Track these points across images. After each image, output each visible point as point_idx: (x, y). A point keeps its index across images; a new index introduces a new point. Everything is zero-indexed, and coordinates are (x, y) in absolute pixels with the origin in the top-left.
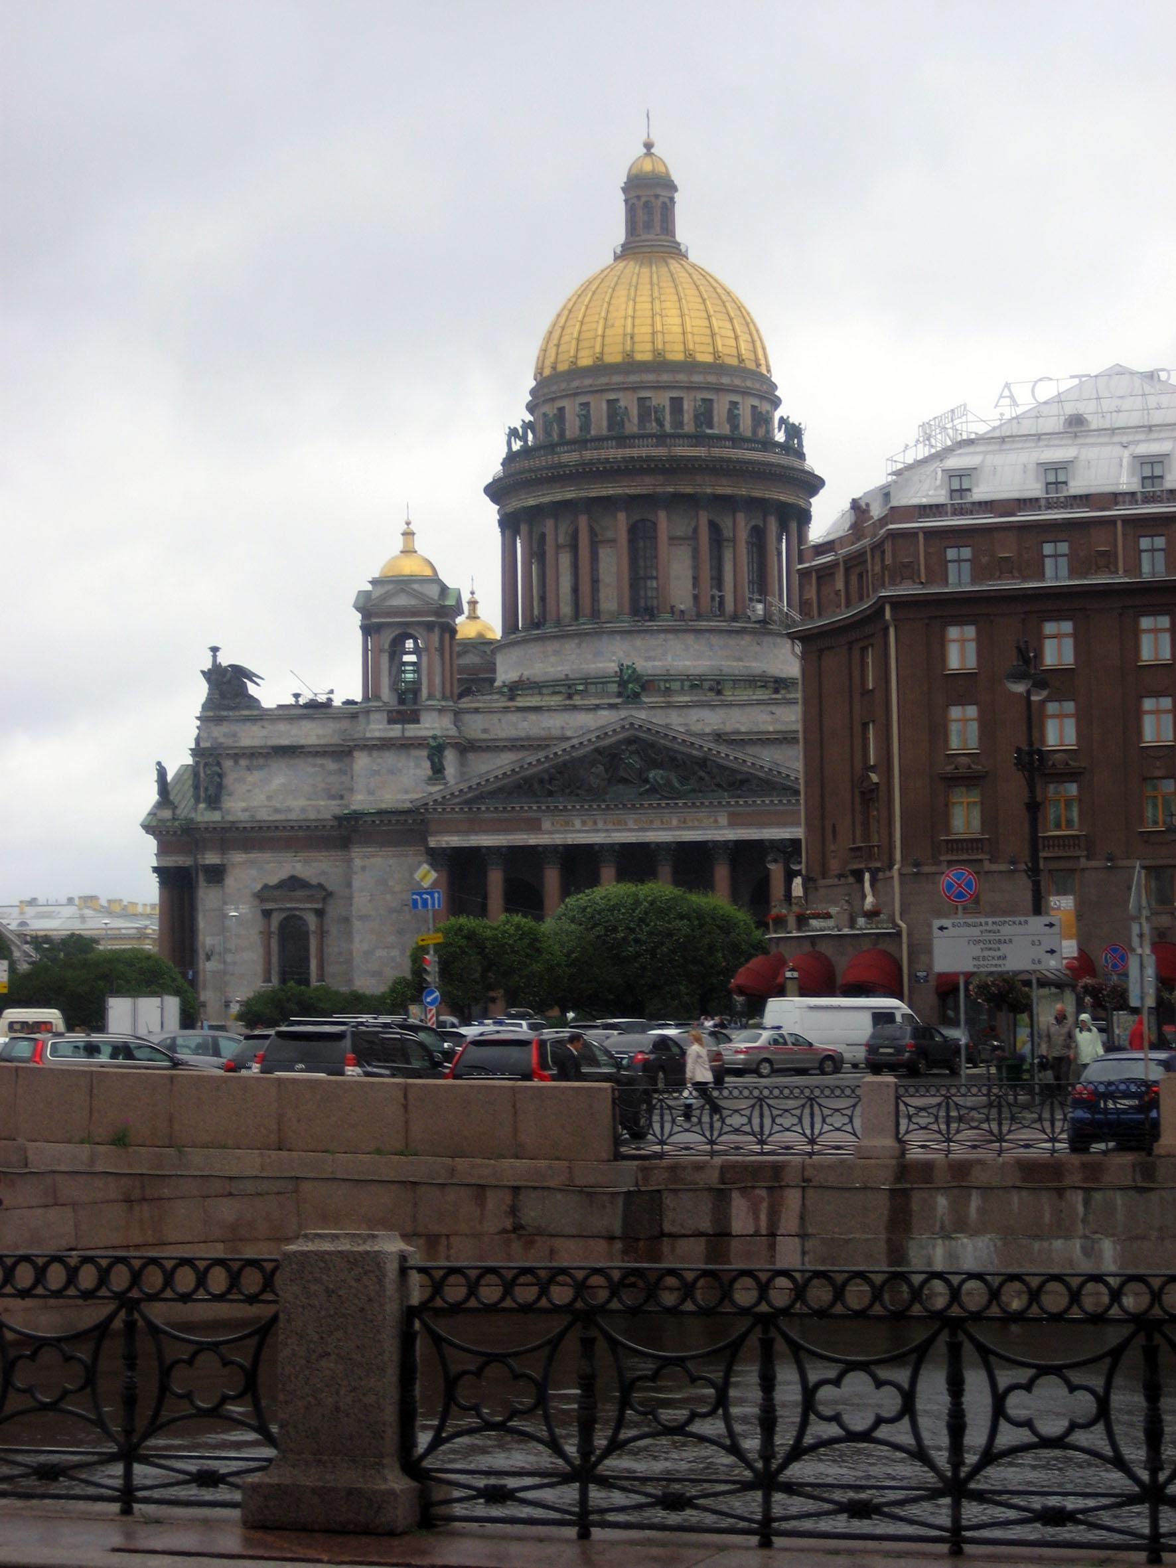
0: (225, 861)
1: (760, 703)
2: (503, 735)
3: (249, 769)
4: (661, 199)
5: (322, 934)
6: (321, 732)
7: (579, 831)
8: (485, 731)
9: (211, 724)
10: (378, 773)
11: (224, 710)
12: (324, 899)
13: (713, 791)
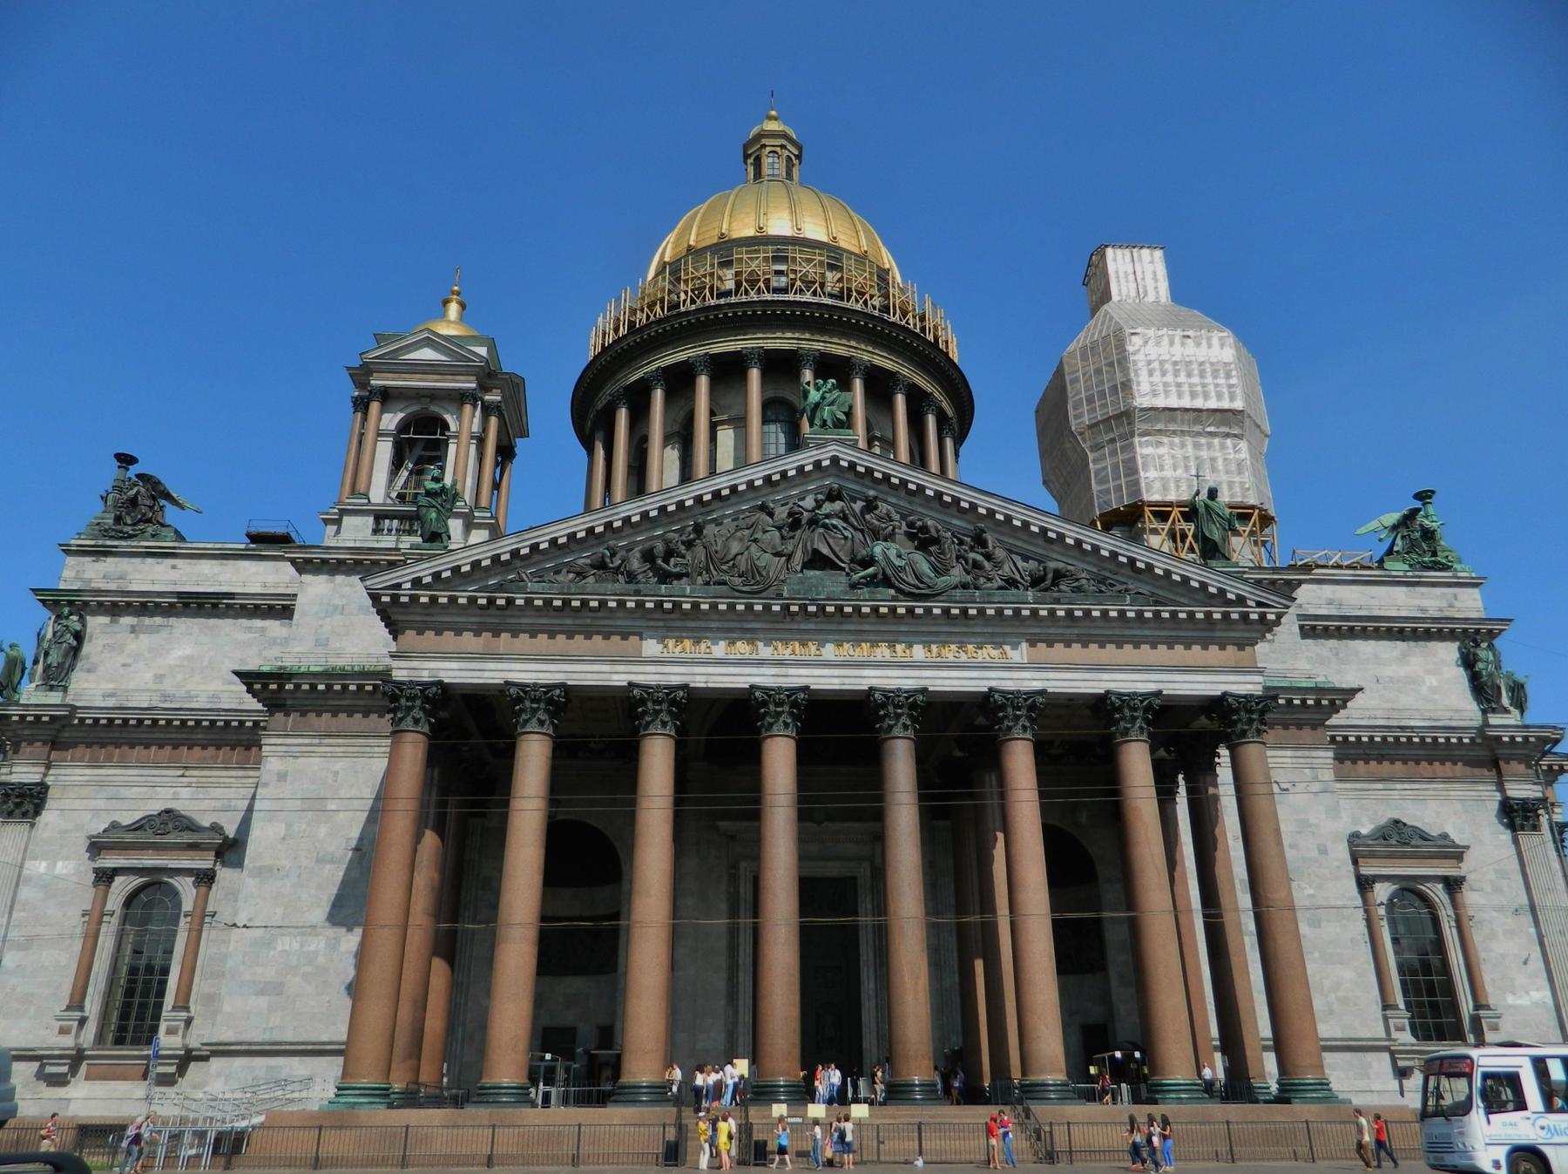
0: (49, 780)
3: (133, 629)
5: (202, 916)
6: (271, 579)
9: (88, 559)
10: (342, 610)
11: (111, 538)
13: (1000, 588)
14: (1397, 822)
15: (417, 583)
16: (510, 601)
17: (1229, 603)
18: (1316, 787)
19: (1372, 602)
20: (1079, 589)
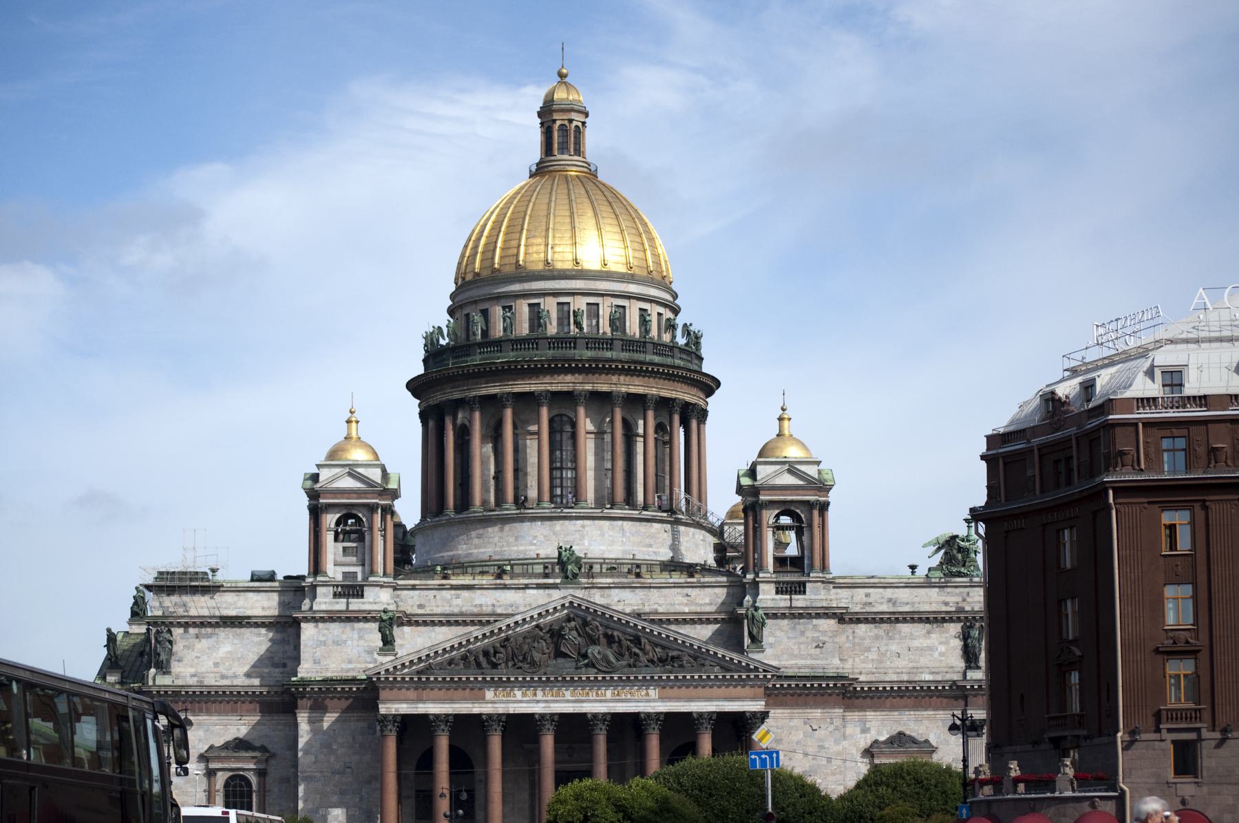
1: (676, 586)
2: (439, 610)
4: (575, 123)
6: (266, 604)
7: (521, 702)
8: (420, 606)
12: (267, 761)
14: (901, 734)
15: (387, 670)
16: (428, 679)
17: (751, 670)
18: (831, 728)
19: (917, 600)
20: (681, 666)
